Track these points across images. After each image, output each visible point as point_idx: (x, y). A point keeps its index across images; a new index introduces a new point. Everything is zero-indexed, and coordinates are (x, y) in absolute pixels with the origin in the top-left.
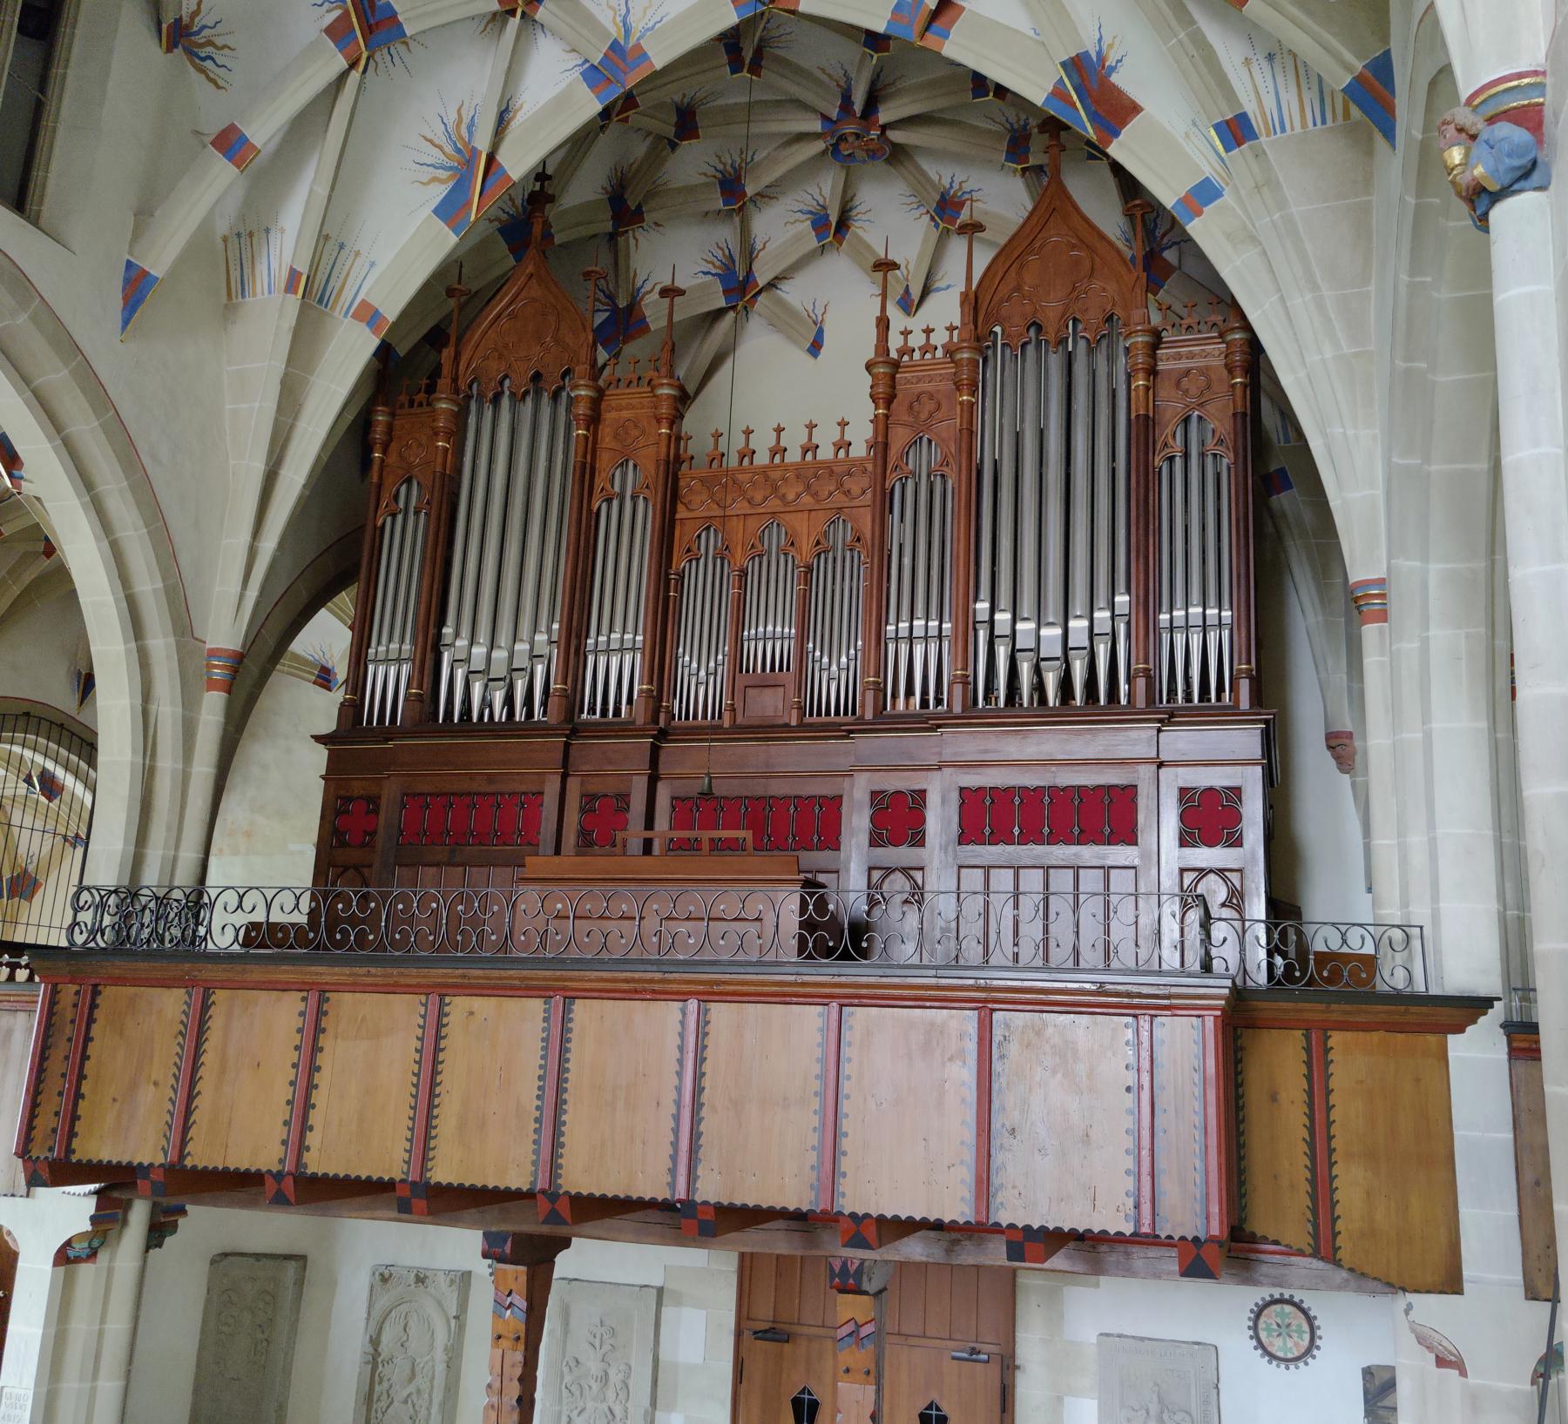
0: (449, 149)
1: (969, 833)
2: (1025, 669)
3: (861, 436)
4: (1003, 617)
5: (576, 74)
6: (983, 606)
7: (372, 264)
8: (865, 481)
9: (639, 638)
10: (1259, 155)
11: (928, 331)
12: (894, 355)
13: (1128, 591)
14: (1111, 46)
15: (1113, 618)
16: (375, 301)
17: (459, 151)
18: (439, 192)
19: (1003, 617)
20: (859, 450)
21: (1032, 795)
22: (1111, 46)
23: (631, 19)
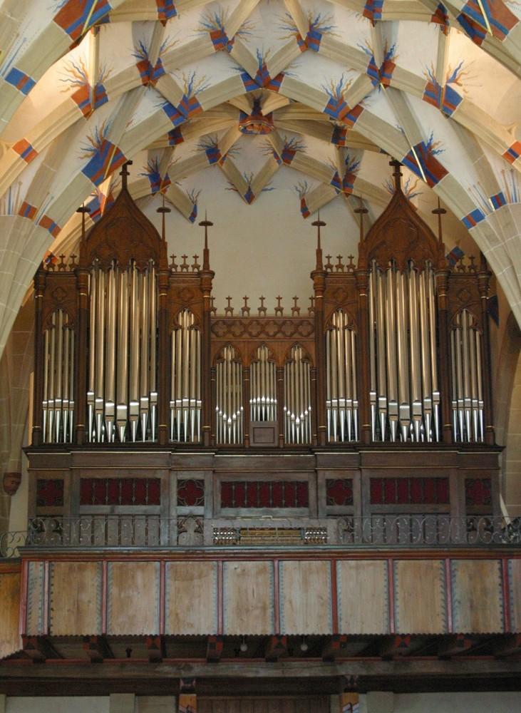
0: (95, 142)
1: (375, 499)
2: (393, 424)
3: (305, 306)
4: (383, 399)
5: (160, 108)
6: (373, 394)
7: (52, 198)
8: (309, 328)
9: (199, 402)
10: (507, 211)
11: (340, 258)
12: (324, 269)
13: (439, 390)
14: (437, 144)
15: (432, 401)
16: (51, 216)
17: (98, 142)
18: (87, 161)
19: (383, 399)
20: (304, 311)
21: (403, 481)
22: (437, 144)
23: (193, 85)
